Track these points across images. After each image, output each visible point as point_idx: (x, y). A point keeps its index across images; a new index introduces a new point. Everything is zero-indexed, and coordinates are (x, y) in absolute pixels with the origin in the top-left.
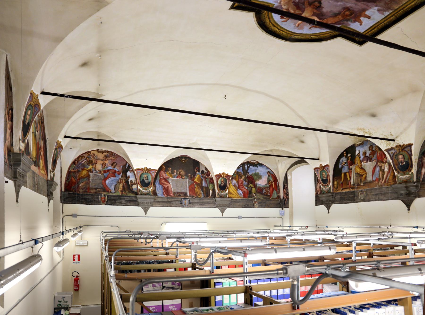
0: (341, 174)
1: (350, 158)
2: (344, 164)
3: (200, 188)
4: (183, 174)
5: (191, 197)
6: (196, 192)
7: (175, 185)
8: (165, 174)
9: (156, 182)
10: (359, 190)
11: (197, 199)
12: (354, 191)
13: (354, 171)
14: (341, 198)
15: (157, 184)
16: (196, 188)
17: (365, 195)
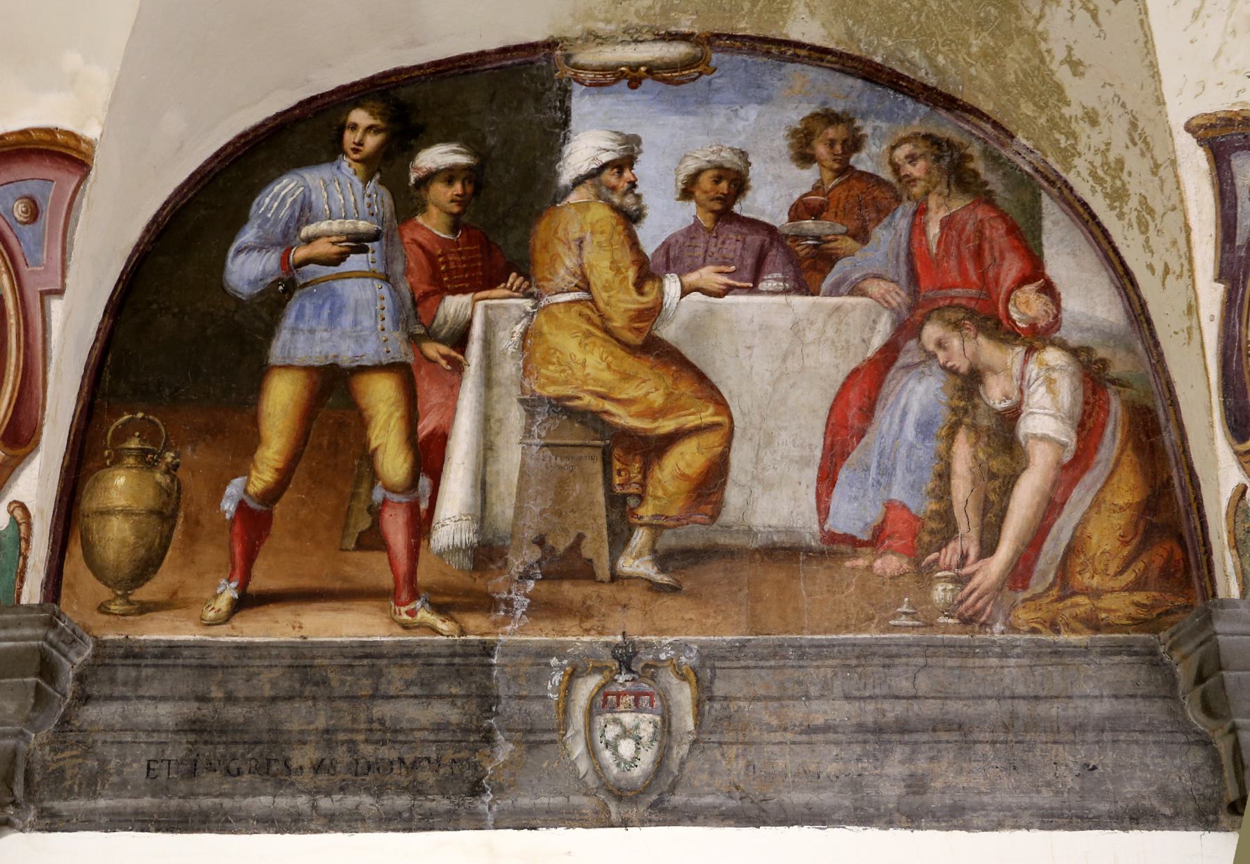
0: (260, 372)
1: (443, 193)
2: (323, 248)
10: (578, 639)
12: (487, 650)
13: (508, 369)
14: (195, 728)
17: (686, 721)
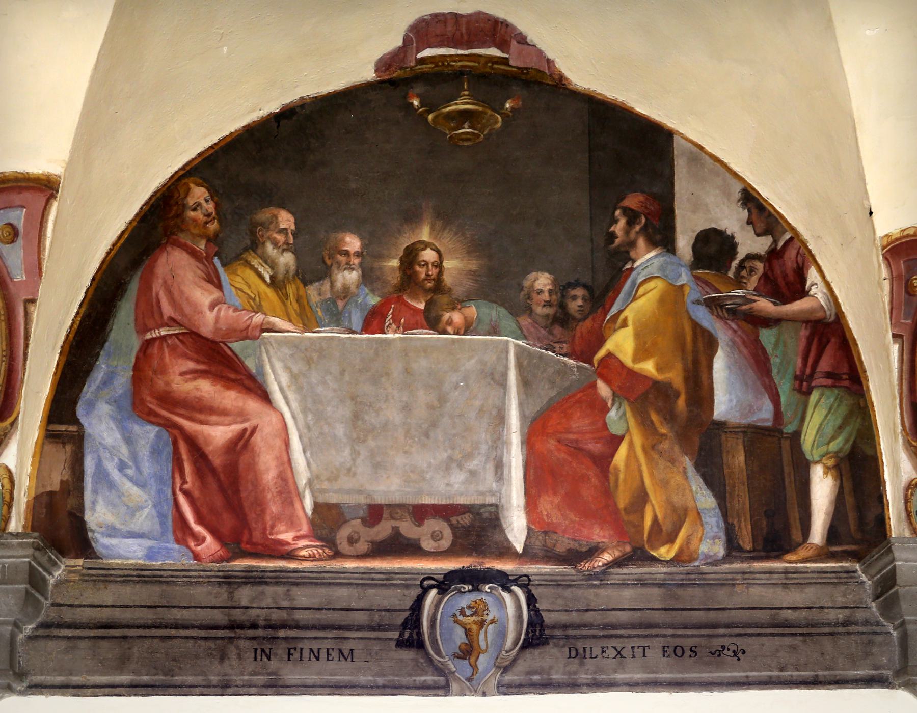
3: (683, 438)
4: (448, 279)
5: (550, 556)
6: (622, 500)
7: (346, 411)
8: (214, 281)
9: (89, 390)
11: (641, 583)
15: (104, 408)
16: (623, 450)
